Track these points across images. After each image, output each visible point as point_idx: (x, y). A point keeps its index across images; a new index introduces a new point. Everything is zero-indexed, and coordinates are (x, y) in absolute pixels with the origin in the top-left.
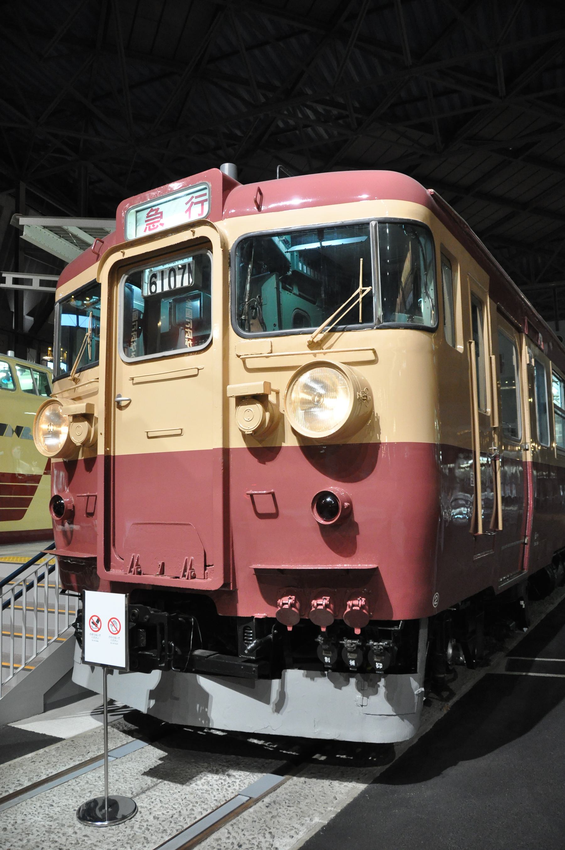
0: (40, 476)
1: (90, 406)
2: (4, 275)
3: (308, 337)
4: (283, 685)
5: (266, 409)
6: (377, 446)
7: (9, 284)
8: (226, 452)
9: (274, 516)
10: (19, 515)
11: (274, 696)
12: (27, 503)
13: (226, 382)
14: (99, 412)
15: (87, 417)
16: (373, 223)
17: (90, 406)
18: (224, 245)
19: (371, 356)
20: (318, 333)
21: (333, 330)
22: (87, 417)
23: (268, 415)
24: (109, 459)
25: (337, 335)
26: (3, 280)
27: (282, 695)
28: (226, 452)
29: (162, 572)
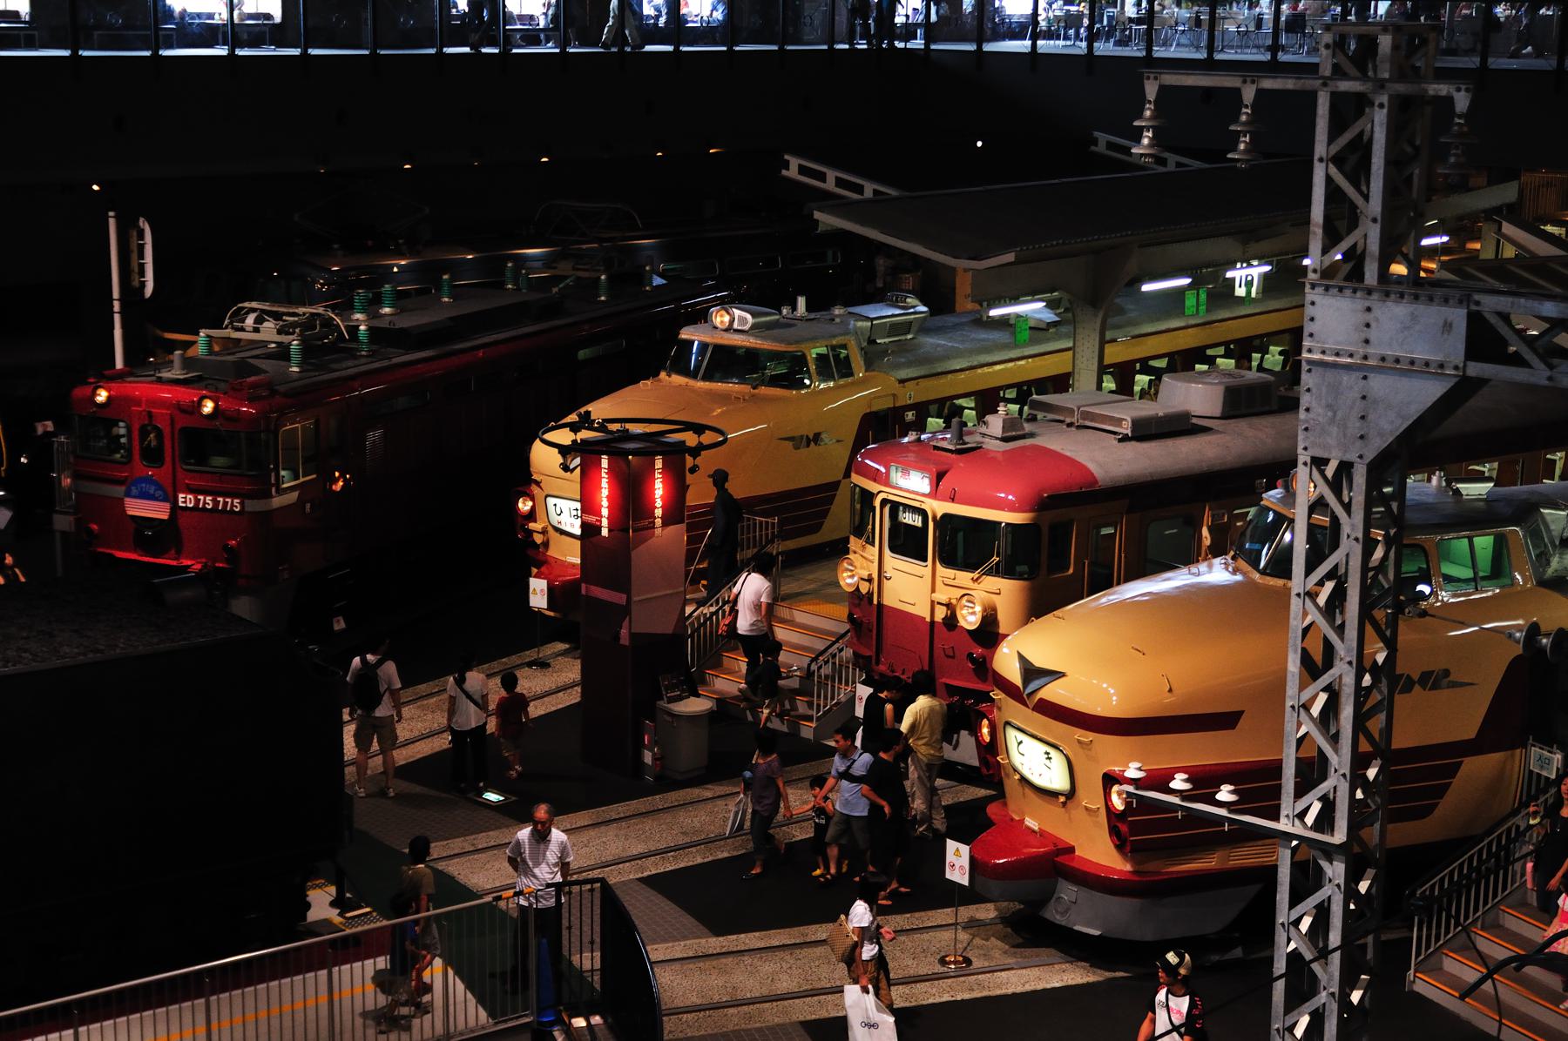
0: (840, 481)
1: (870, 575)
2: (786, 157)
3: (971, 575)
4: (958, 737)
5: (948, 609)
6: (998, 633)
7: (792, 172)
8: (933, 622)
9: (953, 657)
10: (817, 528)
11: (954, 742)
12: (825, 514)
13: (933, 591)
14: (875, 576)
15: (870, 580)
16: (1003, 524)
17: (870, 575)
18: (934, 518)
19: (998, 591)
20: (976, 575)
21: (983, 574)
22: (870, 580)
23: (949, 612)
24: (880, 606)
25: (984, 576)
26: (786, 165)
27: (958, 741)
28: (933, 622)
29: (903, 673)
